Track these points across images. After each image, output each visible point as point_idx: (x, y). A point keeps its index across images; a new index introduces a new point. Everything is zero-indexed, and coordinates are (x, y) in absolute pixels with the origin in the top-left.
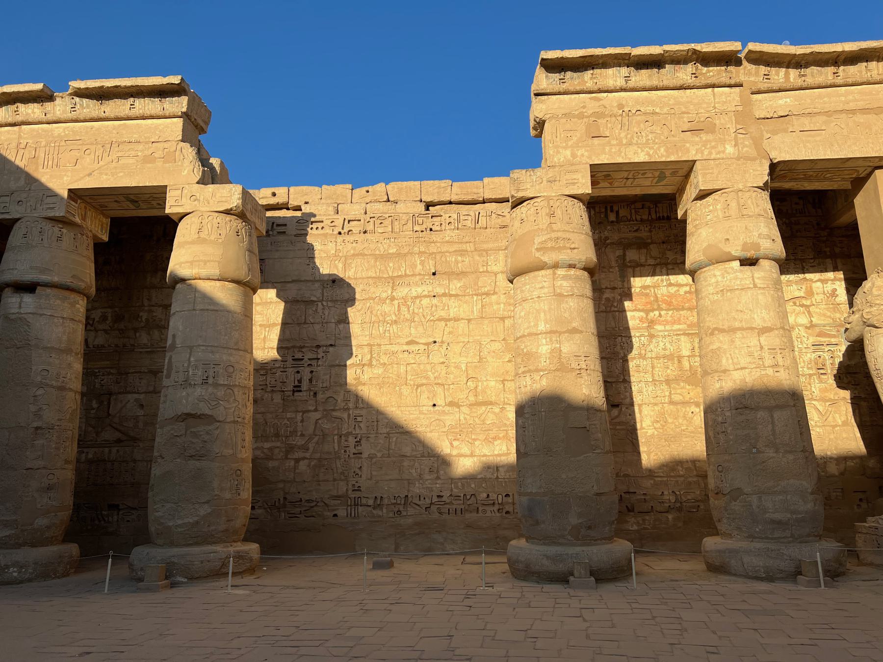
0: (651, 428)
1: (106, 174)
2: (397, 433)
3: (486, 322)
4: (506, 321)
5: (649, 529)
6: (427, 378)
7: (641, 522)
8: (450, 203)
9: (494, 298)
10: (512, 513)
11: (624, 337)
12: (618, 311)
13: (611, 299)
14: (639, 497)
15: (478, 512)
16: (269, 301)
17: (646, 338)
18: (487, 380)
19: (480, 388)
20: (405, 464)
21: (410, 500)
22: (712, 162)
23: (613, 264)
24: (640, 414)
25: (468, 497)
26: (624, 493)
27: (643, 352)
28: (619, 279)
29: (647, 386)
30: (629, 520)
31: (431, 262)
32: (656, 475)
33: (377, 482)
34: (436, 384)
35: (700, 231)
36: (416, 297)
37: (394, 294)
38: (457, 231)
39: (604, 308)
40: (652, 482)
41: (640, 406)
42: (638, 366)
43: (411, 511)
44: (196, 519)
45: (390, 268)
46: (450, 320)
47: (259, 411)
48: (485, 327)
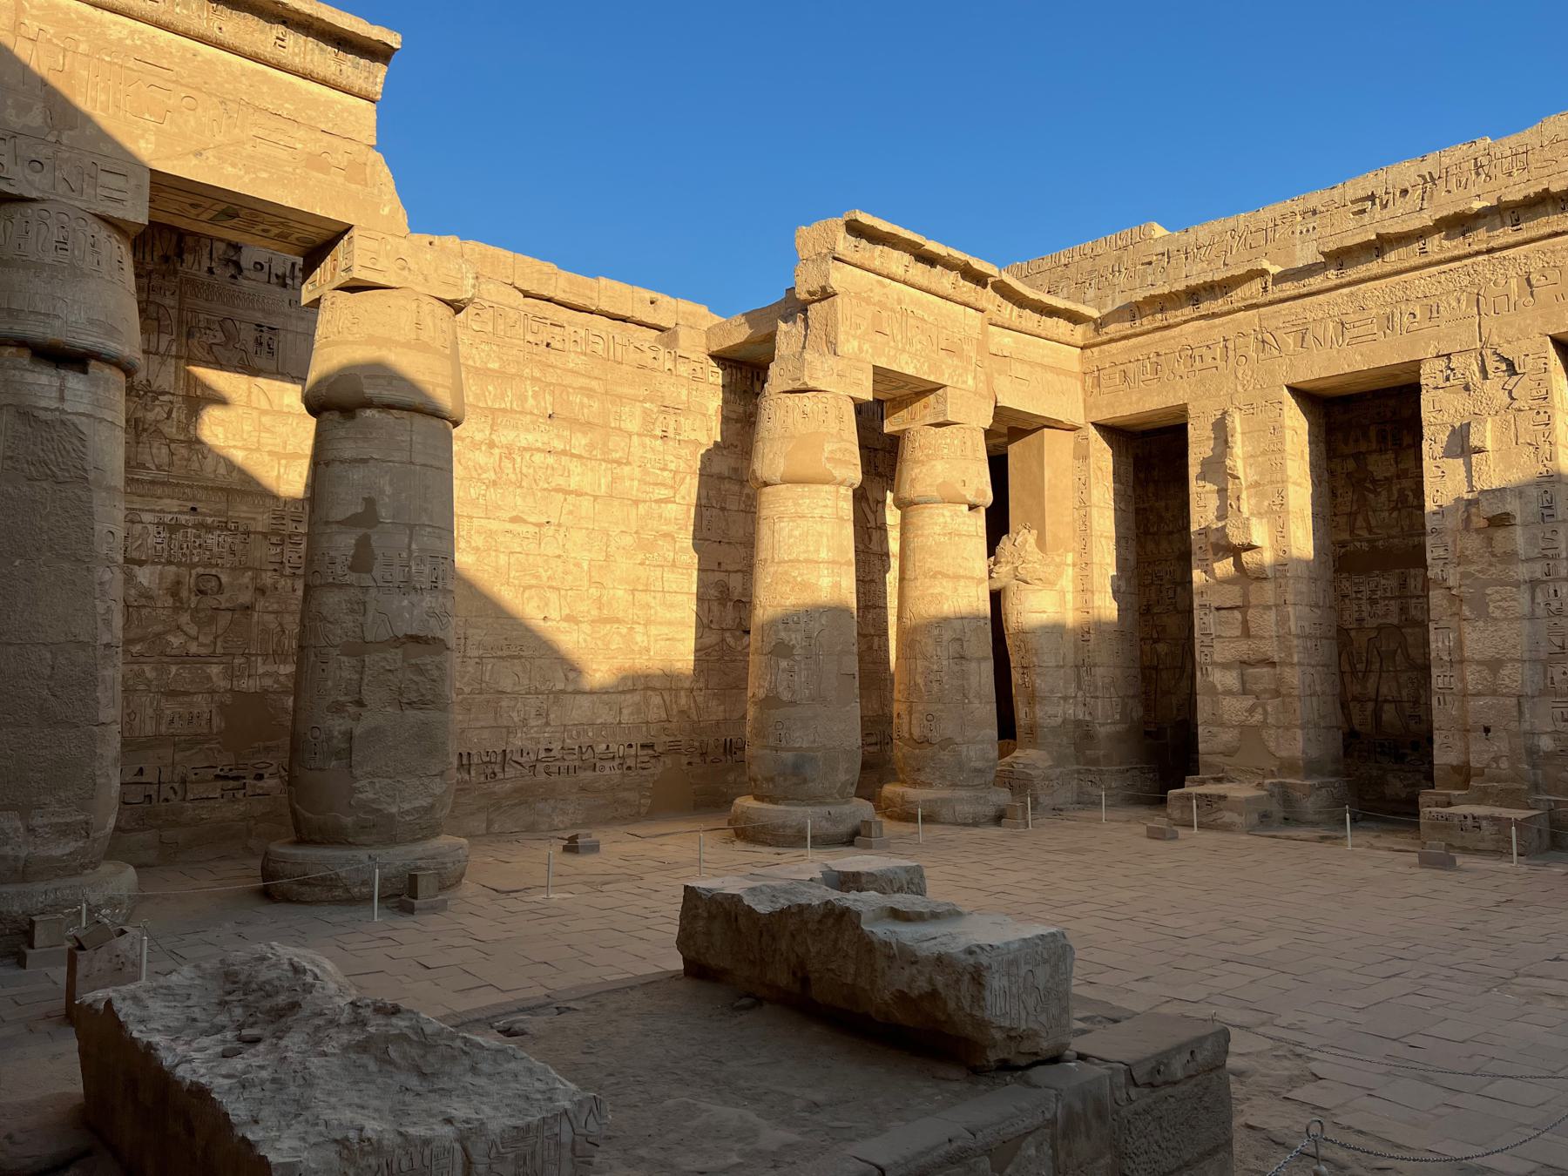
1: (234, 165)
2: (493, 657)
3: (616, 503)
6: (538, 577)
8: (549, 300)
9: (627, 469)
15: (594, 770)
16: (285, 410)
18: (614, 588)
19: (605, 598)
20: (504, 704)
21: (508, 756)
22: (958, 391)
25: (584, 750)
31: (547, 397)
33: (463, 732)
34: (549, 587)
35: (934, 463)
36: (525, 449)
37: (494, 437)
38: (583, 357)
43: (510, 772)
44: (430, 800)
45: (490, 393)
46: (570, 492)
47: (270, 609)
48: (614, 510)
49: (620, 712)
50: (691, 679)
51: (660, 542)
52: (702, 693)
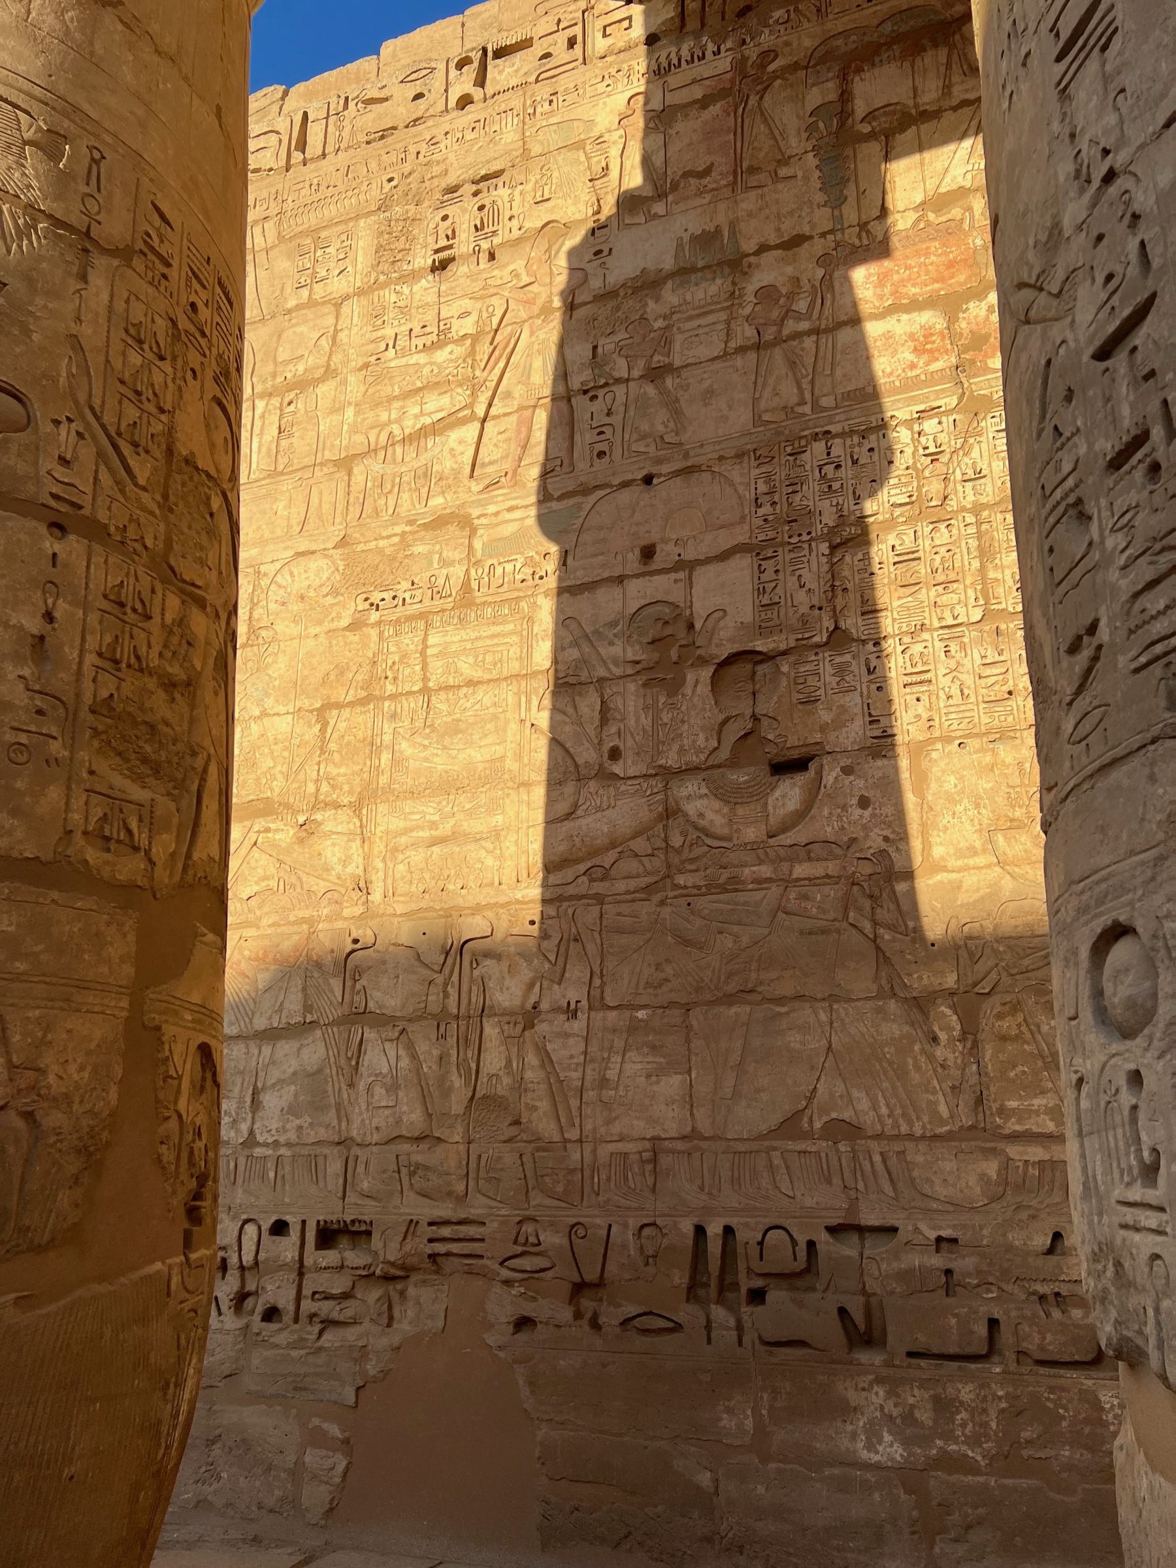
0: (980, 860)
4: (356, 470)
5: (972, 1469)
7: (925, 1416)
10: (288, 1318)
11: (842, 435)
12: (817, 332)
13: (784, 291)
14: (915, 1260)
17: (947, 421)
18: (264, 714)
23: (795, 143)
24: (920, 793)
26: (832, 1230)
27: (934, 488)
28: (820, 197)
29: (953, 647)
30: (853, 1397)
32: (1013, 1126)
39: (750, 332)
40: (991, 1168)
41: (920, 749)
42: (909, 558)
49: (256, 1104)
50: (526, 974)
51: (419, 549)
52: (578, 1026)
